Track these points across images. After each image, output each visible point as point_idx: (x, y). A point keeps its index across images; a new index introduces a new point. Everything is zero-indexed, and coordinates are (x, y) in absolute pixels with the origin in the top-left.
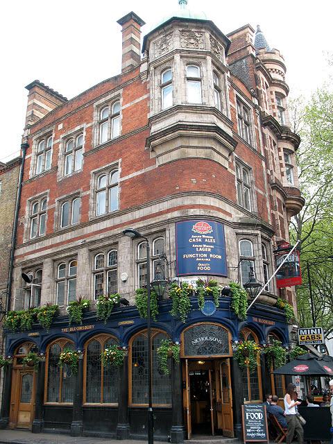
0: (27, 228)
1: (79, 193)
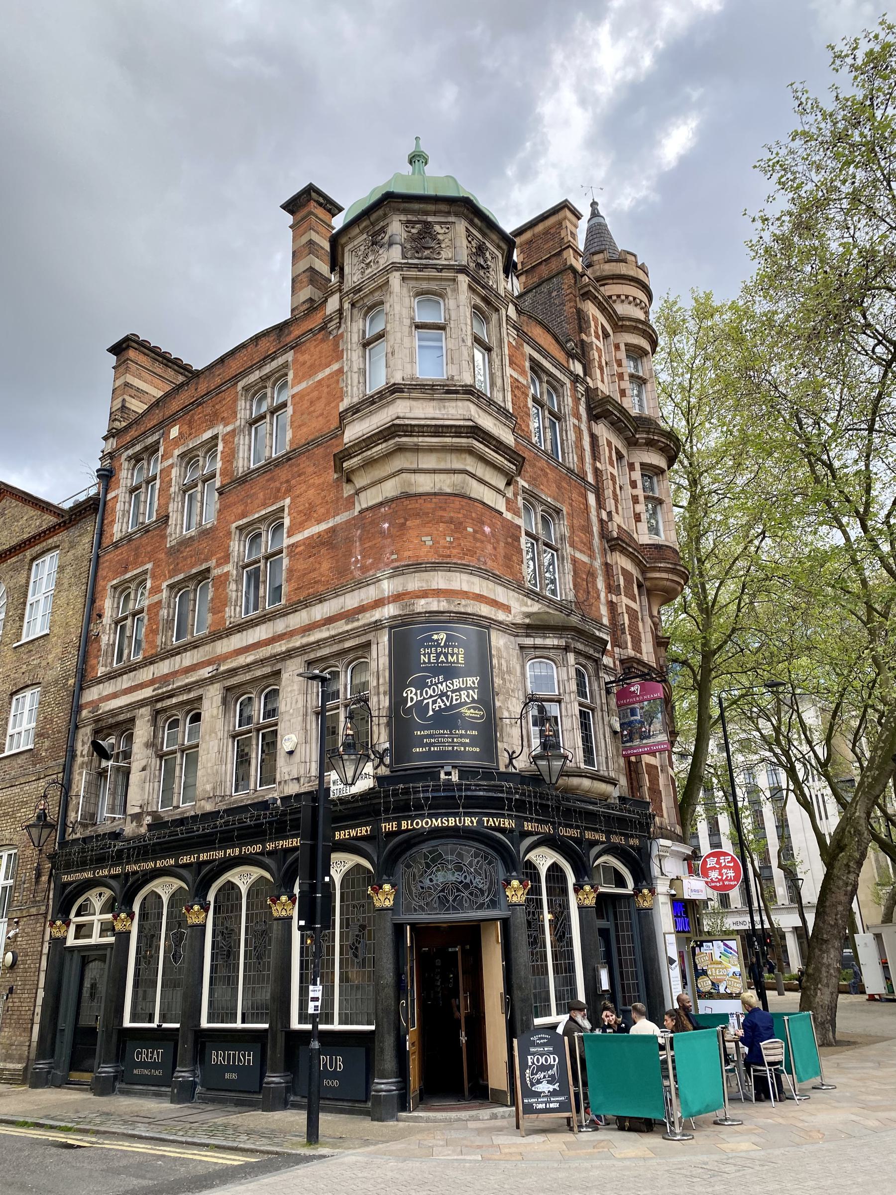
0: (108, 645)
1: (208, 570)
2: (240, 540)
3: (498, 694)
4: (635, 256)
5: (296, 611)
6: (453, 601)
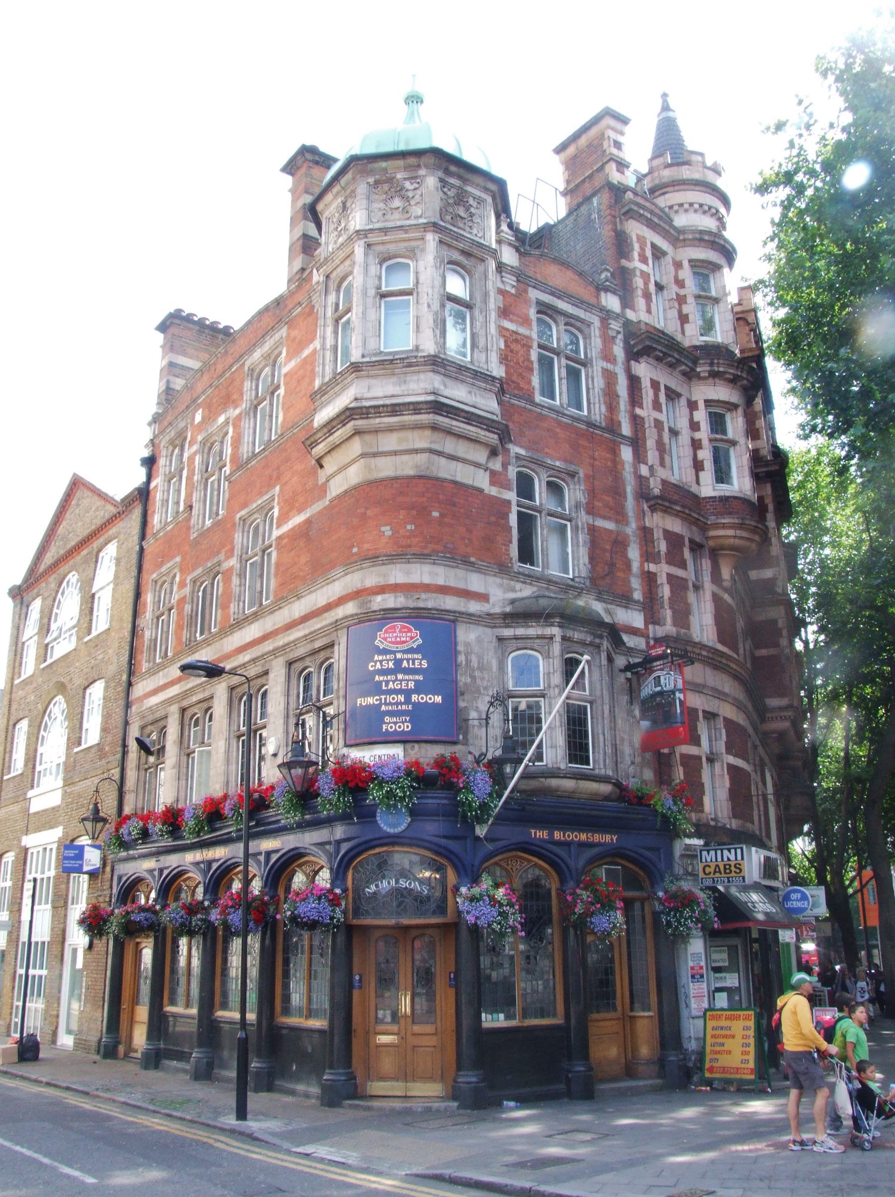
0: (151, 640)
1: (219, 564)
2: (243, 532)
3: (463, 694)
4: (702, 155)
5: (280, 608)
6: (412, 597)
